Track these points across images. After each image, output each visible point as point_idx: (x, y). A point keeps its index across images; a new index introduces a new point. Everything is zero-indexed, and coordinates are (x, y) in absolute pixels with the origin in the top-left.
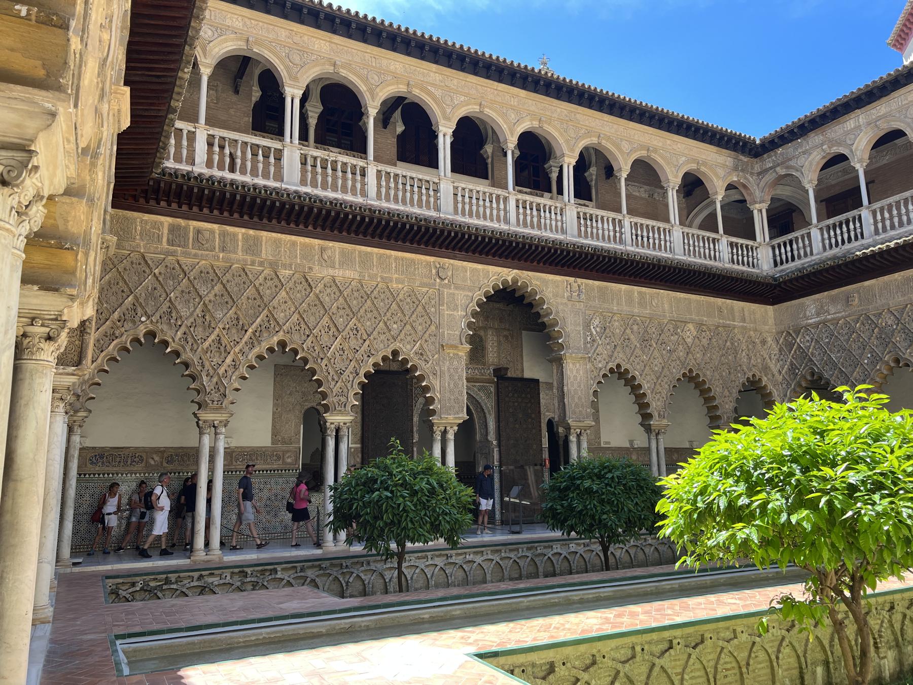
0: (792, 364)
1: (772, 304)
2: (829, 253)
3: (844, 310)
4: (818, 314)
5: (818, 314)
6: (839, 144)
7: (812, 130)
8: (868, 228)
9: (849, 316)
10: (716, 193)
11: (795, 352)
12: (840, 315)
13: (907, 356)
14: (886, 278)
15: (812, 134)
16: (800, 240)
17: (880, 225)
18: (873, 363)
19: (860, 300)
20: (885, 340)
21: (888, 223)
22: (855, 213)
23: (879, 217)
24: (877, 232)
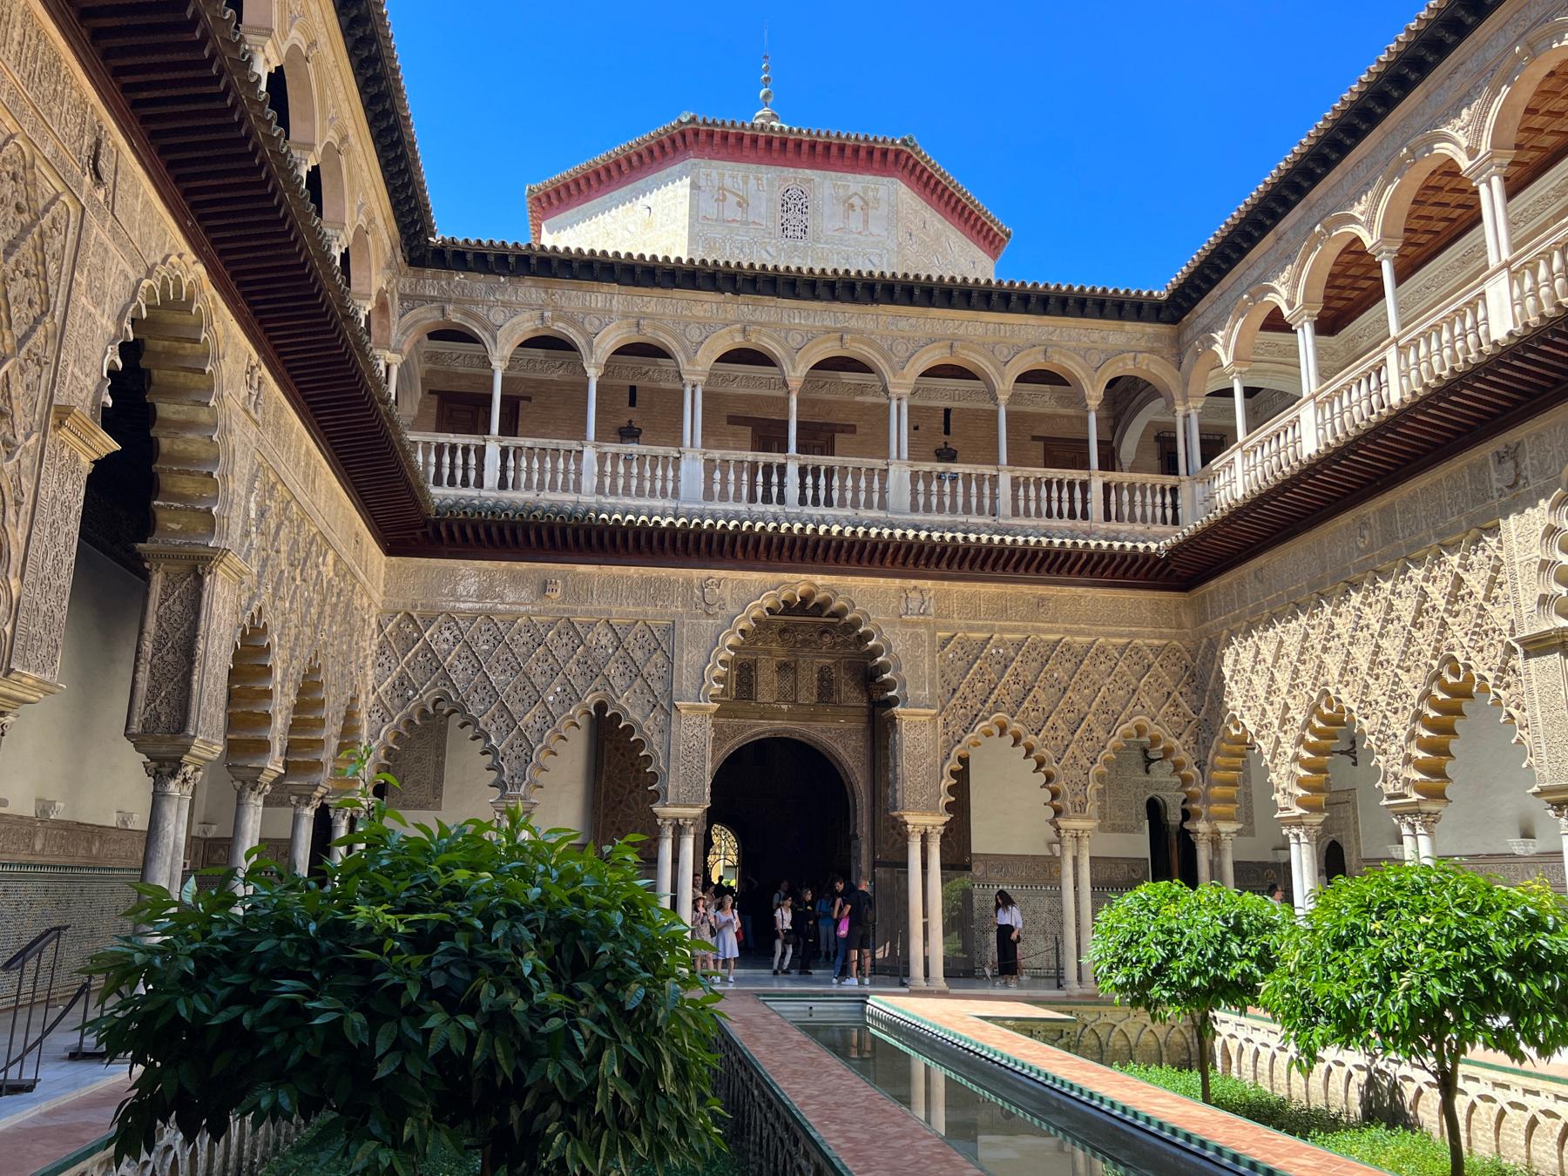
0: (401, 678)
1: (389, 552)
2: (509, 495)
3: (532, 603)
4: (481, 597)
5: (481, 597)
6: (571, 321)
7: (534, 274)
8: (589, 481)
9: (540, 613)
10: (368, 297)
11: (416, 655)
12: (523, 609)
13: (621, 702)
14: (616, 570)
15: (528, 281)
16: (459, 453)
17: (608, 481)
18: (565, 703)
19: (564, 593)
20: (593, 670)
21: (621, 482)
22: (574, 445)
23: (608, 468)
24: (600, 490)
